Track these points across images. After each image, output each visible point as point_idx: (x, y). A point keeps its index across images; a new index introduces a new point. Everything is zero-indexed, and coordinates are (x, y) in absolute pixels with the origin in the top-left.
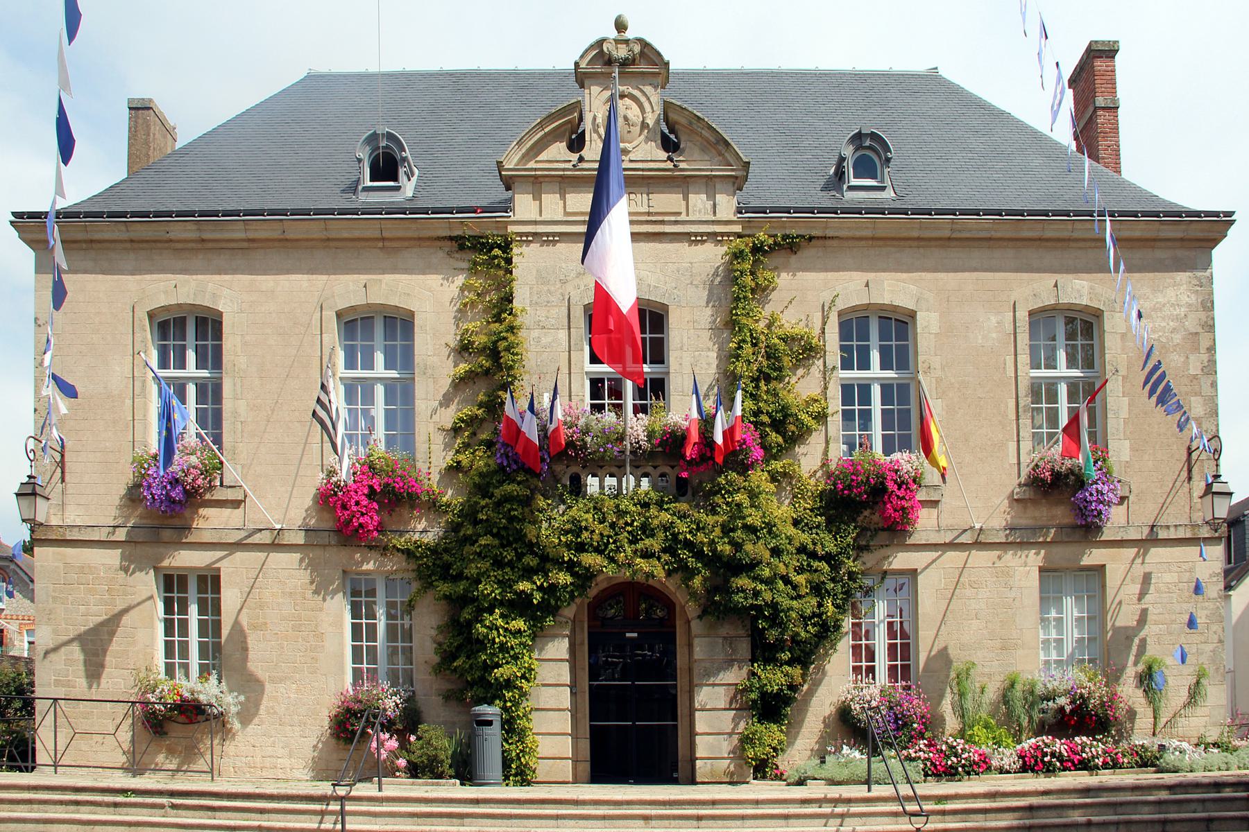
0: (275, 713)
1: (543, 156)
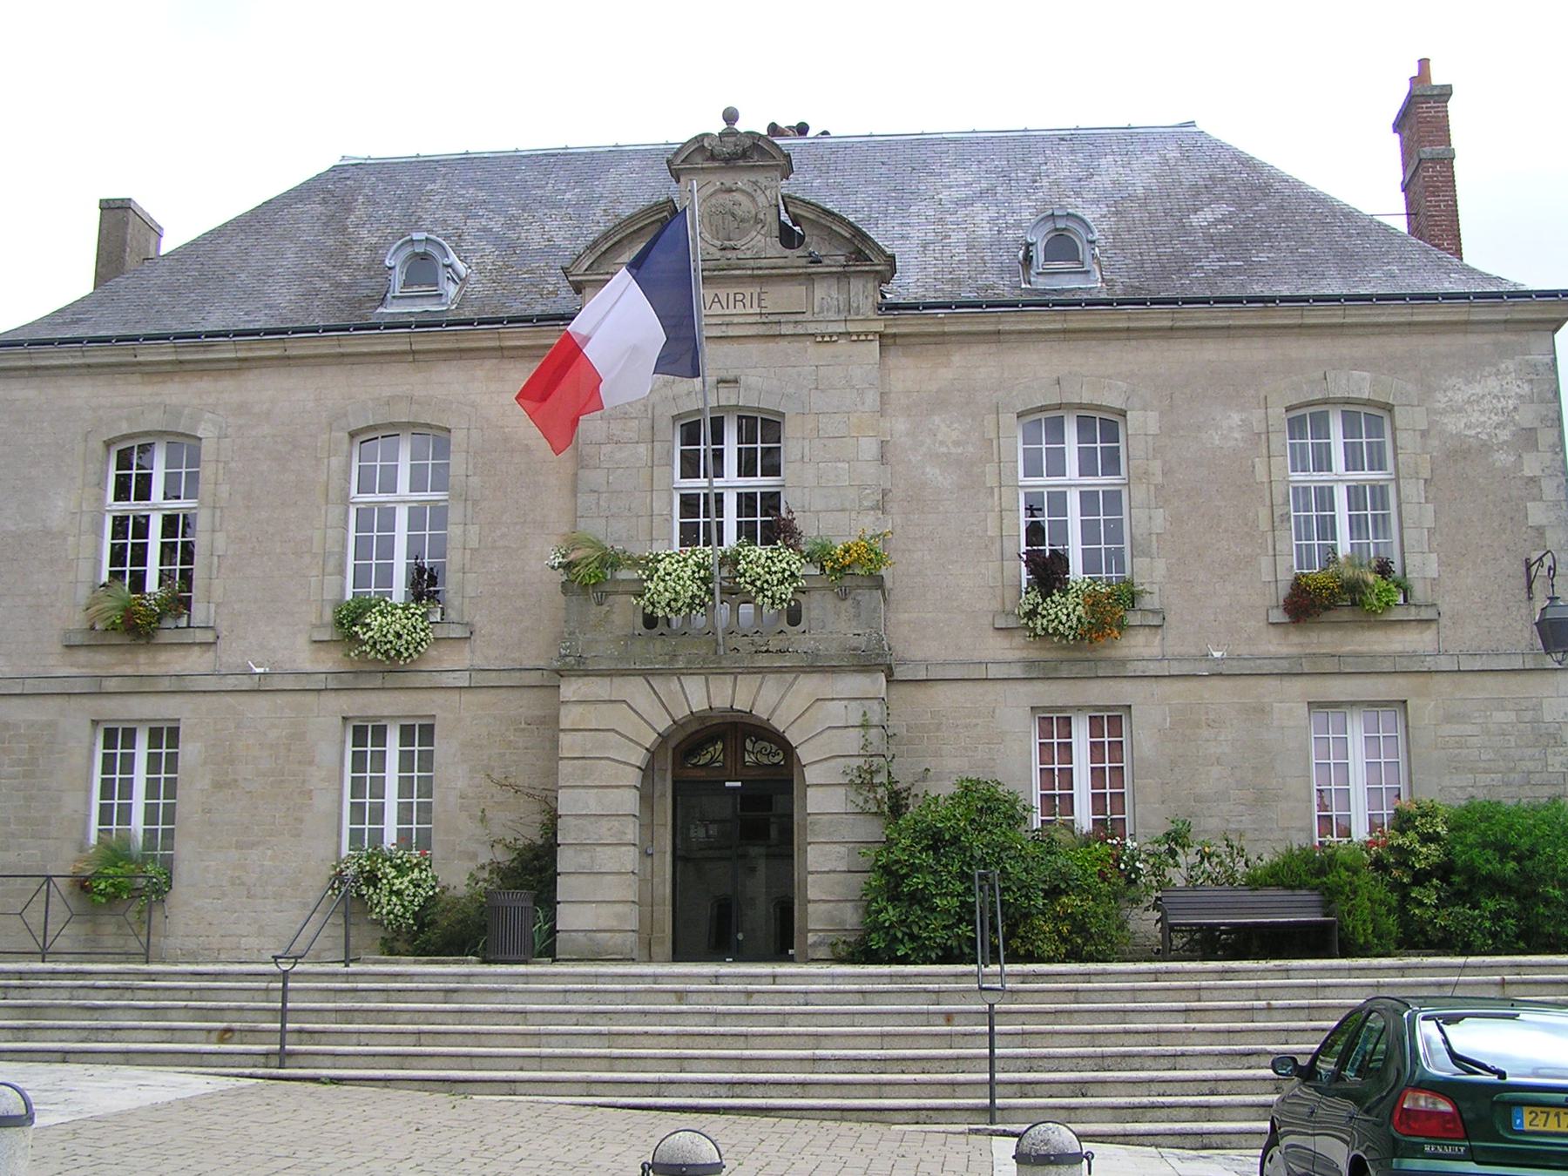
0: (243, 884)
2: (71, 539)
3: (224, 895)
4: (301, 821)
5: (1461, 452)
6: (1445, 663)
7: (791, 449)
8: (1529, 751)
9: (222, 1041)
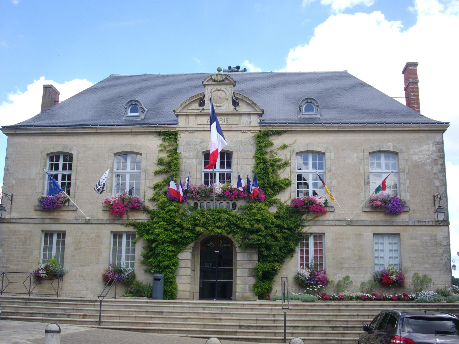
0: (82, 276)
1: (190, 108)
2: (36, 180)
3: (77, 279)
4: (98, 259)
5: (417, 165)
6: (411, 223)
7: (234, 161)
8: (433, 248)
9: (83, 318)
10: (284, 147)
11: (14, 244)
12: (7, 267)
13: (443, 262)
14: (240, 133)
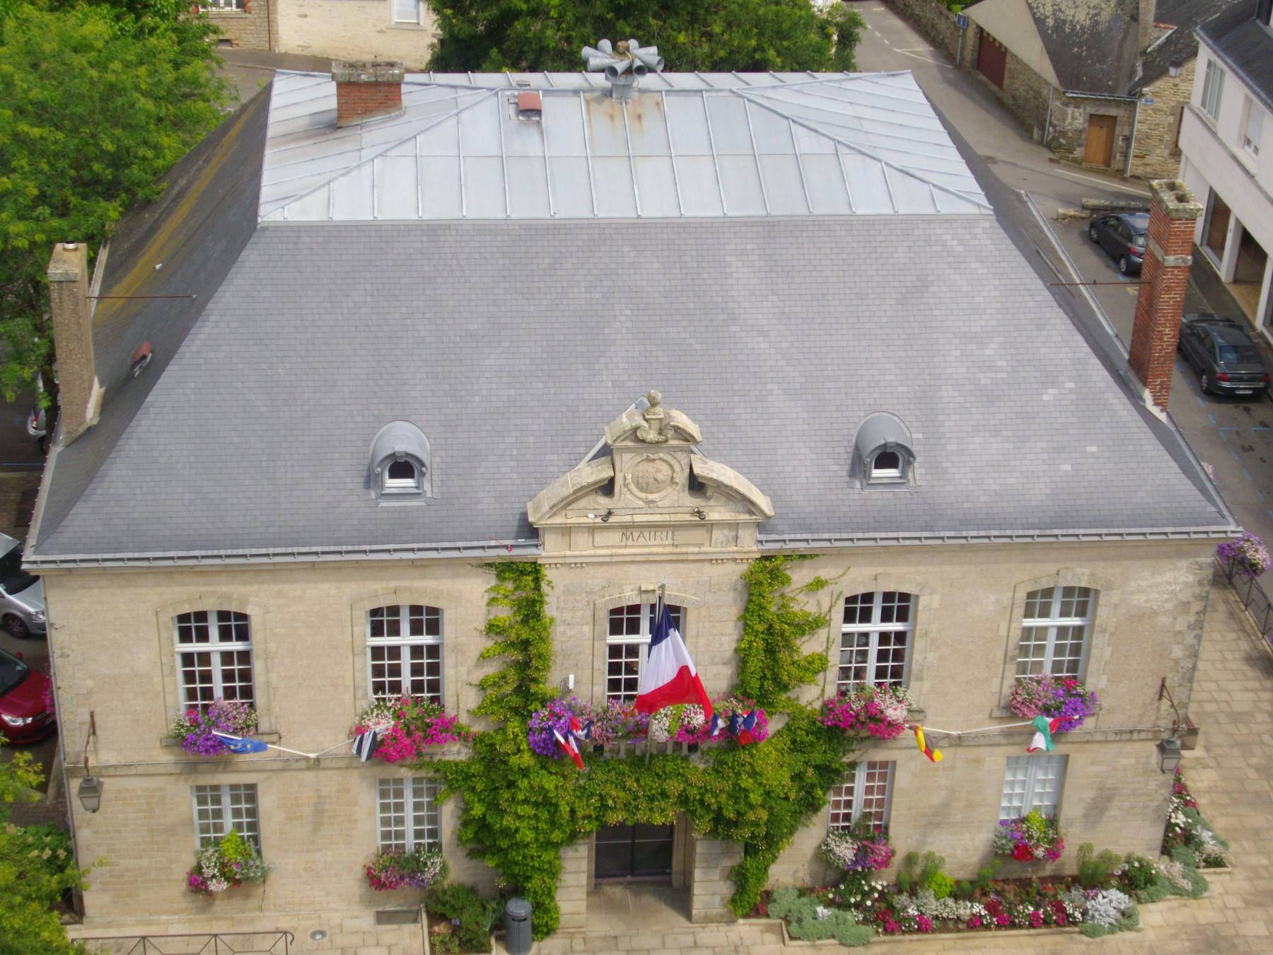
6: (1098, 737)
10: (819, 584)
11: (121, 816)
12: (112, 864)
13: (1156, 803)
14: (707, 565)
